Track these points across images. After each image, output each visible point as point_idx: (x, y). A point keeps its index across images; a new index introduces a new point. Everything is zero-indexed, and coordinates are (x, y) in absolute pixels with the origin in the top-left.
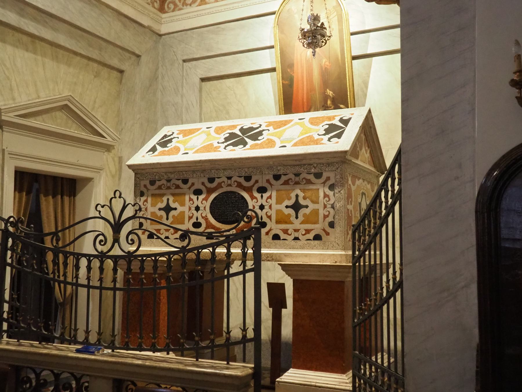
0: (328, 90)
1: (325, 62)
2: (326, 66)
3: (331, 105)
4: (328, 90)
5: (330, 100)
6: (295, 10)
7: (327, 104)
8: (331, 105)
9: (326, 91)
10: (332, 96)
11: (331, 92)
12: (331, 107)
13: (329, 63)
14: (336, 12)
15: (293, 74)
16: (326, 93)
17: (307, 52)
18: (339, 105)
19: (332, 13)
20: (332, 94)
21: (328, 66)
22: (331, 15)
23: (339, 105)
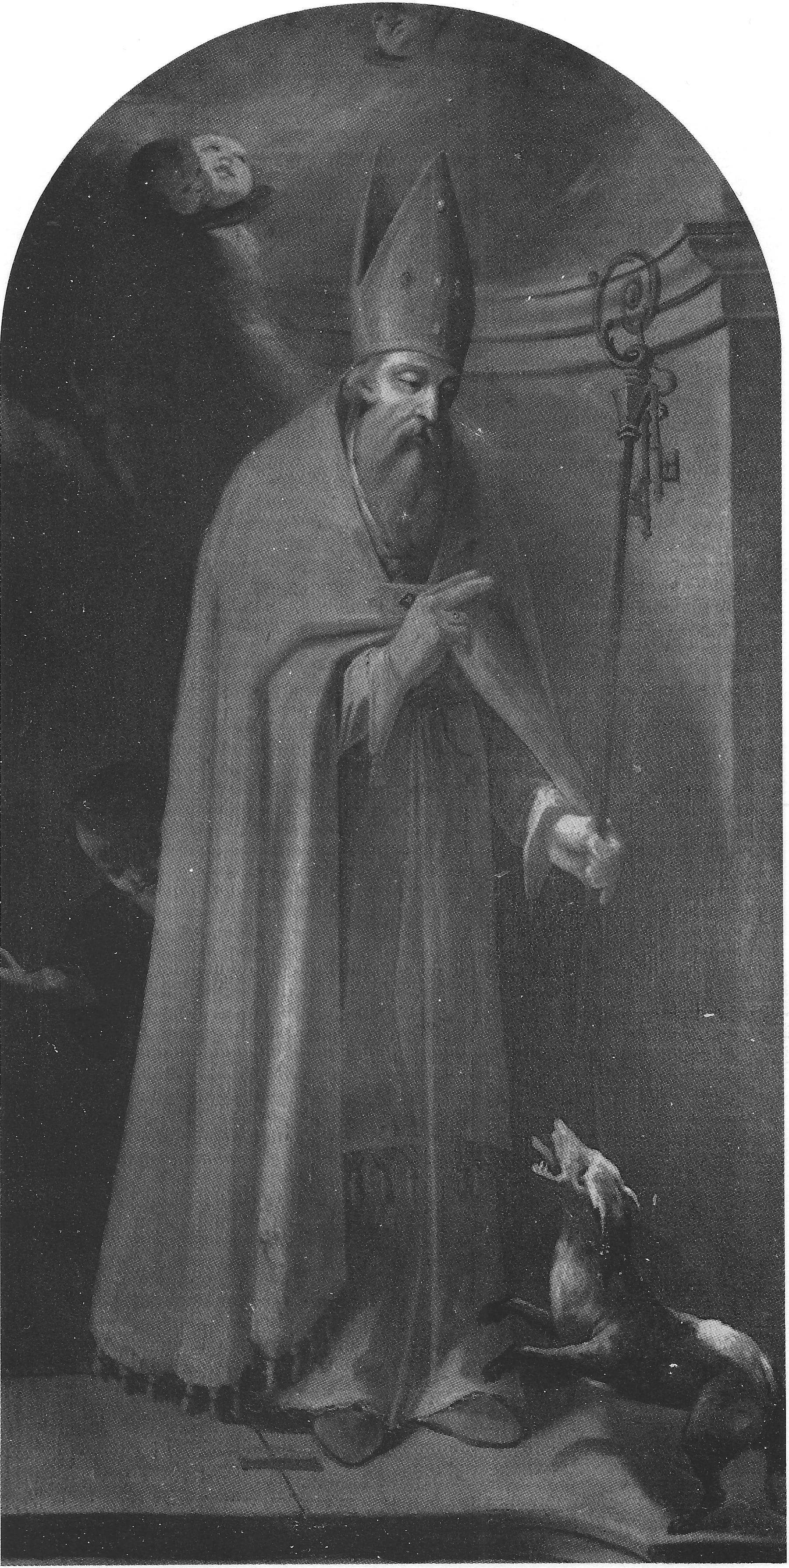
0: (561, 1129)
1: (552, 816)
2: (557, 856)
3: (587, 1311)
4: (561, 1129)
5: (585, 1254)
6: (225, 170)
7: (547, 1302)
8: (587, 1311)
9: (550, 1145)
10: (609, 1199)
11: (598, 1161)
12: (585, 1333)
13: (601, 830)
14: (714, 293)
15: (143, 899)
16: (539, 1169)
17: (343, 663)
18: (686, 1317)
19: (666, 296)
20: (603, 1181)
21: (580, 853)
22: (657, 310)
23: (686, 1317)
